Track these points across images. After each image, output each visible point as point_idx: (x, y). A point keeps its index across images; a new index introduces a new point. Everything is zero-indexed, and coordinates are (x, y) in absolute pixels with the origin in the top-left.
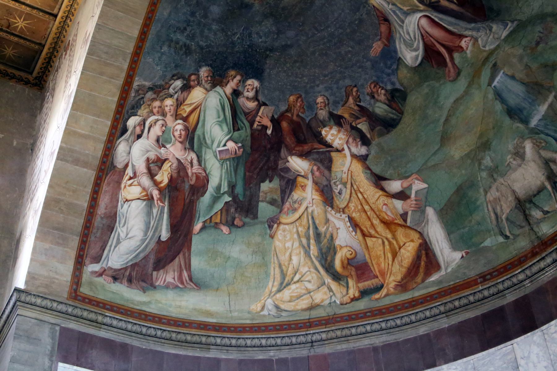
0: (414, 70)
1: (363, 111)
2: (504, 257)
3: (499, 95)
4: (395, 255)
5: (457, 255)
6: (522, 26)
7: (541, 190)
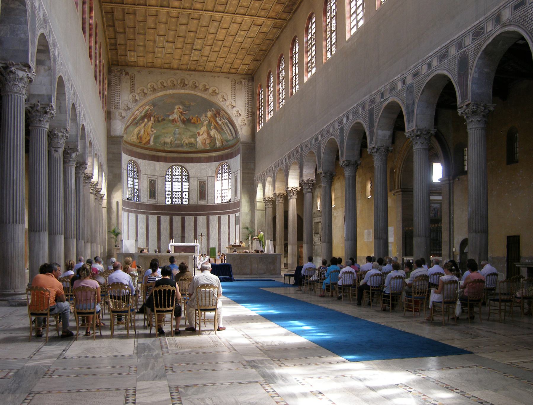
0: (169, 119)
1: (158, 118)
2: (158, 148)
7: (168, 143)
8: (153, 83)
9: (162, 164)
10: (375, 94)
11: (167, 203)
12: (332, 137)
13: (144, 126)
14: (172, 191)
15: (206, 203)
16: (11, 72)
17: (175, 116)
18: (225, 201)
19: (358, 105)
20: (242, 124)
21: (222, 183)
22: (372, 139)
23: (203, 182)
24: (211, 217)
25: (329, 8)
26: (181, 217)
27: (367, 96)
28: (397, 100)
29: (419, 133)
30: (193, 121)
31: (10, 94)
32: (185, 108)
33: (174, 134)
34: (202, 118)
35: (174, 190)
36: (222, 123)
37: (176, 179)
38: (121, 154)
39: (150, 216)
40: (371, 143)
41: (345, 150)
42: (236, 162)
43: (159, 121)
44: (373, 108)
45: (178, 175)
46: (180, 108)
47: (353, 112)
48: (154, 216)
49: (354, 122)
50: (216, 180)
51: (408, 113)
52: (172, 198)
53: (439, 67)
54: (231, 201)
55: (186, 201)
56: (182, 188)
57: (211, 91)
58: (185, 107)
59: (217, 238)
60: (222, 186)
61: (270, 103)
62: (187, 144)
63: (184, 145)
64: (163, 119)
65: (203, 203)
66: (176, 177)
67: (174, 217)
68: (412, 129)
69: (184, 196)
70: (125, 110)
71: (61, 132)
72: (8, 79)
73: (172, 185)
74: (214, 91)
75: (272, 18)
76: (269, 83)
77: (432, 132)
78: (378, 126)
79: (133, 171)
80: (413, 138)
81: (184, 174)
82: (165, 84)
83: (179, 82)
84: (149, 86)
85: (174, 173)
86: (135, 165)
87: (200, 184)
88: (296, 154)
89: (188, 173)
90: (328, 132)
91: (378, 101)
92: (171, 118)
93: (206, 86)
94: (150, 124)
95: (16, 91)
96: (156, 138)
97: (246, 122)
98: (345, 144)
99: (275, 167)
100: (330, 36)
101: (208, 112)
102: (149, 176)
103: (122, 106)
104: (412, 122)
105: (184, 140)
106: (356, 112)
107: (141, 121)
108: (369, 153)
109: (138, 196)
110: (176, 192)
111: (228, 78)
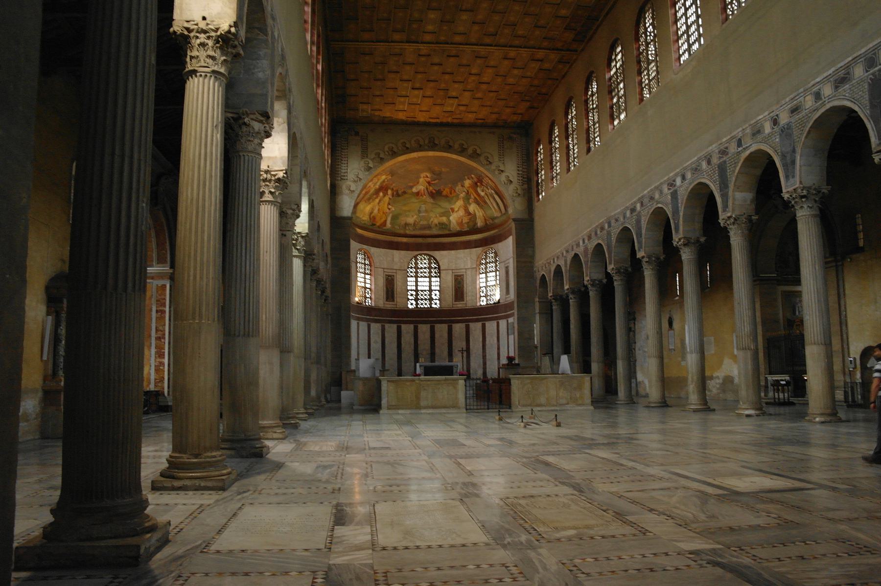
1: (397, 191)
3: (420, 207)
4: (381, 219)
5: (390, 226)
6: (436, 204)
8: (391, 145)
9: (403, 252)
10: (728, 141)
11: (410, 307)
12: (660, 205)
13: (379, 203)
14: (417, 291)
15: (464, 305)
16: (245, 124)
17: (421, 187)
18: (492, 302)
19: (699, 159)
20: (515, 195)
21: (487, 277)
22: (725, 207)
23: (460, 276)
24: (472, 325)
25: (642, 30)
26: (429, 325)
27: (714, 146)
28: (764, 147)
29: (805, 192)
30: (444, 193)
31: (241, 154)
32: (435, 176)
33: (419, 211)
34: (457, 189)
35: (419, 288)
36: (486, 194)
37: (421, 272)
38: (349, 241)
39: (387, 326)
40: (724, 211)
41: (681, 222)
42: (508, 247)
43: (398, 195)
44: (725, 162)
45: (425, 268)
46: (427, 177)
47: (692, 169)
48: (392, 325)
49: (695, 183)
50: (478, 273)
51: (785, 165)
52: (416, 300)
53: (835, 96)
54: (501, 301)
55: (436, 304)
56: (430, 286)
57: (470, 151)
58: (434, 174)
59: (481, 354)
60: (487, 281)
61: (554, 163)
62: (436, 225)
63: (433, 226)
64: (405, 193)
65: (460, 305)
66: (422, 270)
67: (420, 326)
68: (794, 188)
69: (433, 297)
70: (355, 181)
71: (291, 209)
72: (240, 133)
73: (417, 281)
74: (475, 151)
75: (557, 49)
76: (551, 137)
77: (823, 191)
78: (735, 185)
79: (365, 264)
80: (797, 200)
81: (433, 265)
82: (408, 145)
83: (427, 142)
84: (386, 149)
85: (420, 266)
86: (367, 255)
87: (456, 280)
88: (601, 232)
89: (439, 265)
90: (652, 198)
91: (733, 151)
92: (414, 190)
93: (463, 145)
94: (387, 199)
95: (250, 150)
96: (395, 218)
97: (519, 192)
98: (681, 214)
99: (567, 251)
100: (647, 69)
101: (465, 180)
102: (385, 270)
103: (351, 176)
104: (793, 177)
105: (432, 219)
106: (696, 169)
107: (375, 196)
108: (722, 225)
109: (371, 298)
110: (422, 291)
111: (494, 133)
